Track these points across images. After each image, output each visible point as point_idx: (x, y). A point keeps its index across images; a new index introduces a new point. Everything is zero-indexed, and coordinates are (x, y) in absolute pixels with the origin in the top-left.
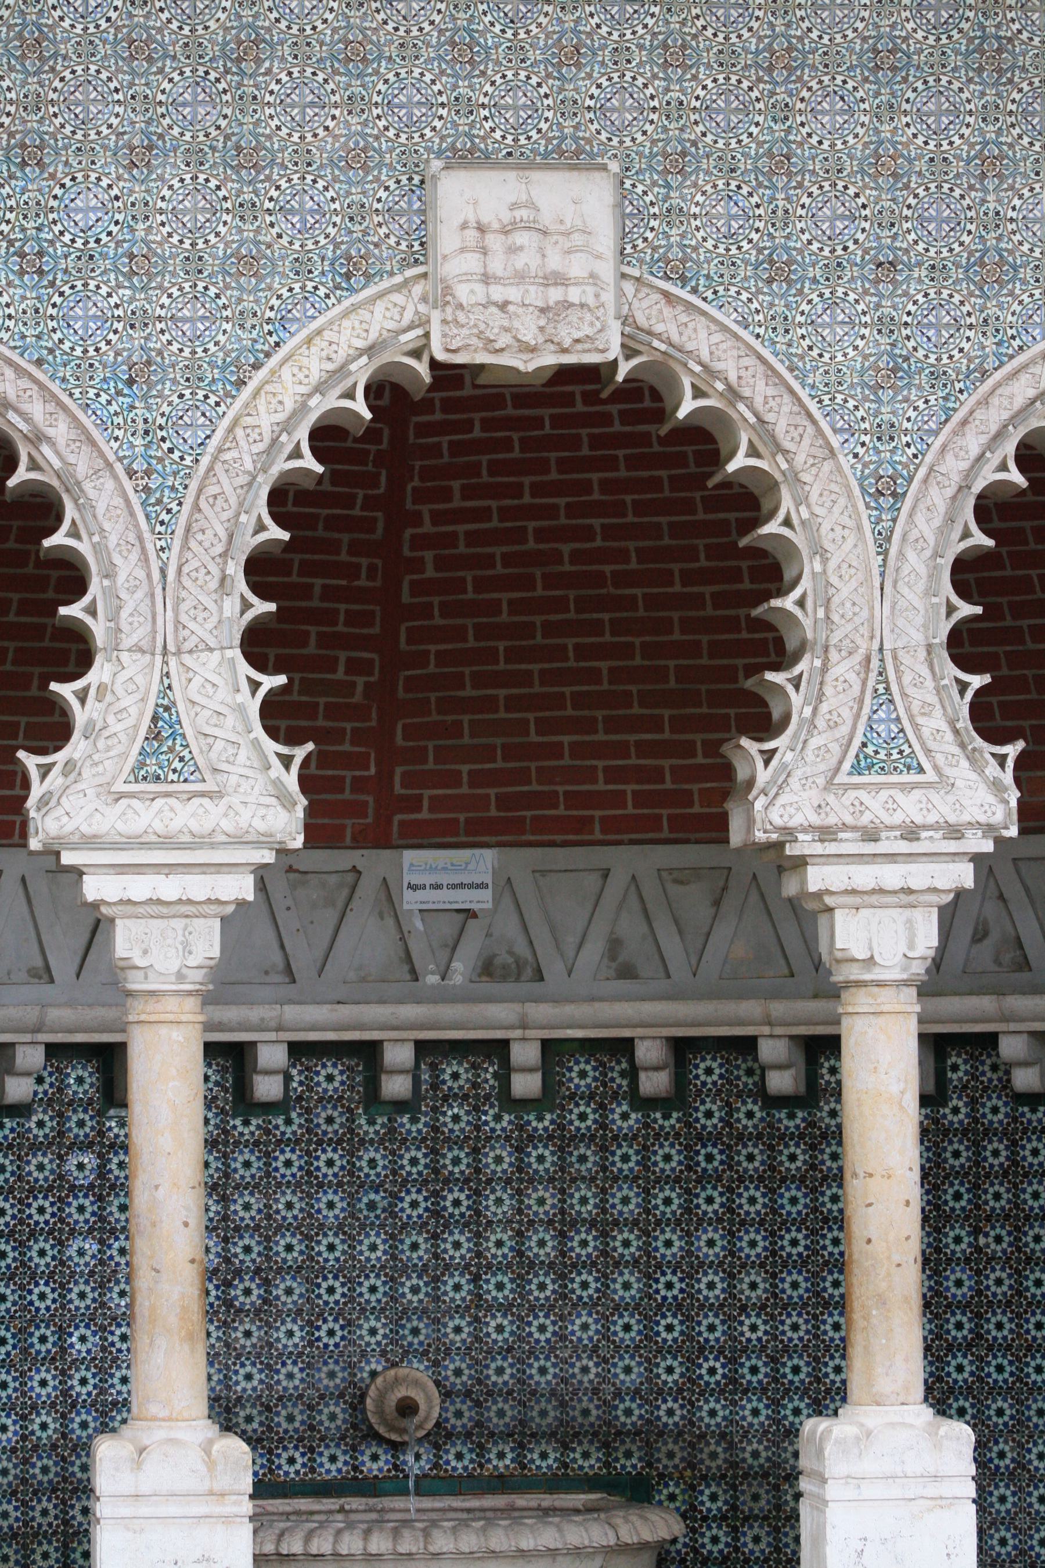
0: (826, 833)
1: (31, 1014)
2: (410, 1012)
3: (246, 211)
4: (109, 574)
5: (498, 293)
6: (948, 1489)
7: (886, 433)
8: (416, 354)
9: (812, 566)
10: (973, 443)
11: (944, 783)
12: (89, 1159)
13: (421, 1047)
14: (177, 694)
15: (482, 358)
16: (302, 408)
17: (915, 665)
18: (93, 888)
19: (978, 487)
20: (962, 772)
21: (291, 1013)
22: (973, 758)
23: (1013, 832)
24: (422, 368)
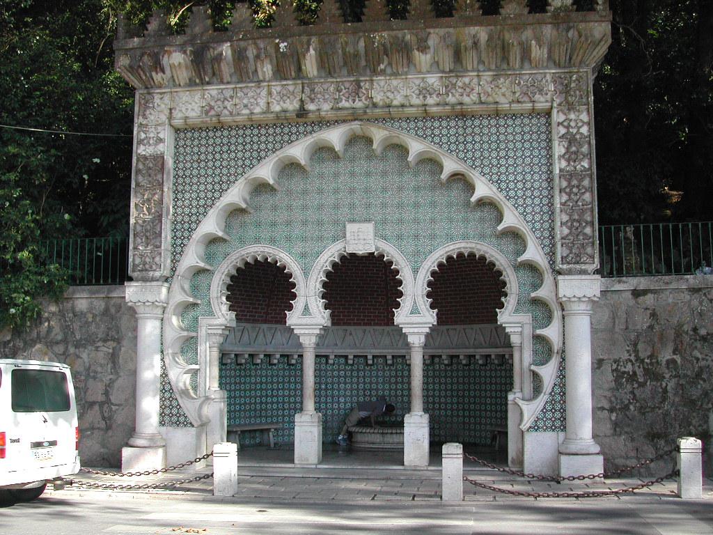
0: (403, 324)
1: (330, 351)
2: (390, 351)
3: (320, 231)
4: (299, 284)
5: (356, 242)
6: (423, 425)
7: (416, 262)
8: (345, 251)
9: (404, 282)
10: (429, 264)
11: (424, 316)
12: (343, 372)
13: (335, 356)
14: (309, 305)
15: (354, 252)
16: (327, 260)
17: (420, 298)
18: (295, 332)
19: (430, 270)
20: (427, 314)
21: (372, 351)
22: (429, 312)
23: (435, 323)
24: (345, 254)
